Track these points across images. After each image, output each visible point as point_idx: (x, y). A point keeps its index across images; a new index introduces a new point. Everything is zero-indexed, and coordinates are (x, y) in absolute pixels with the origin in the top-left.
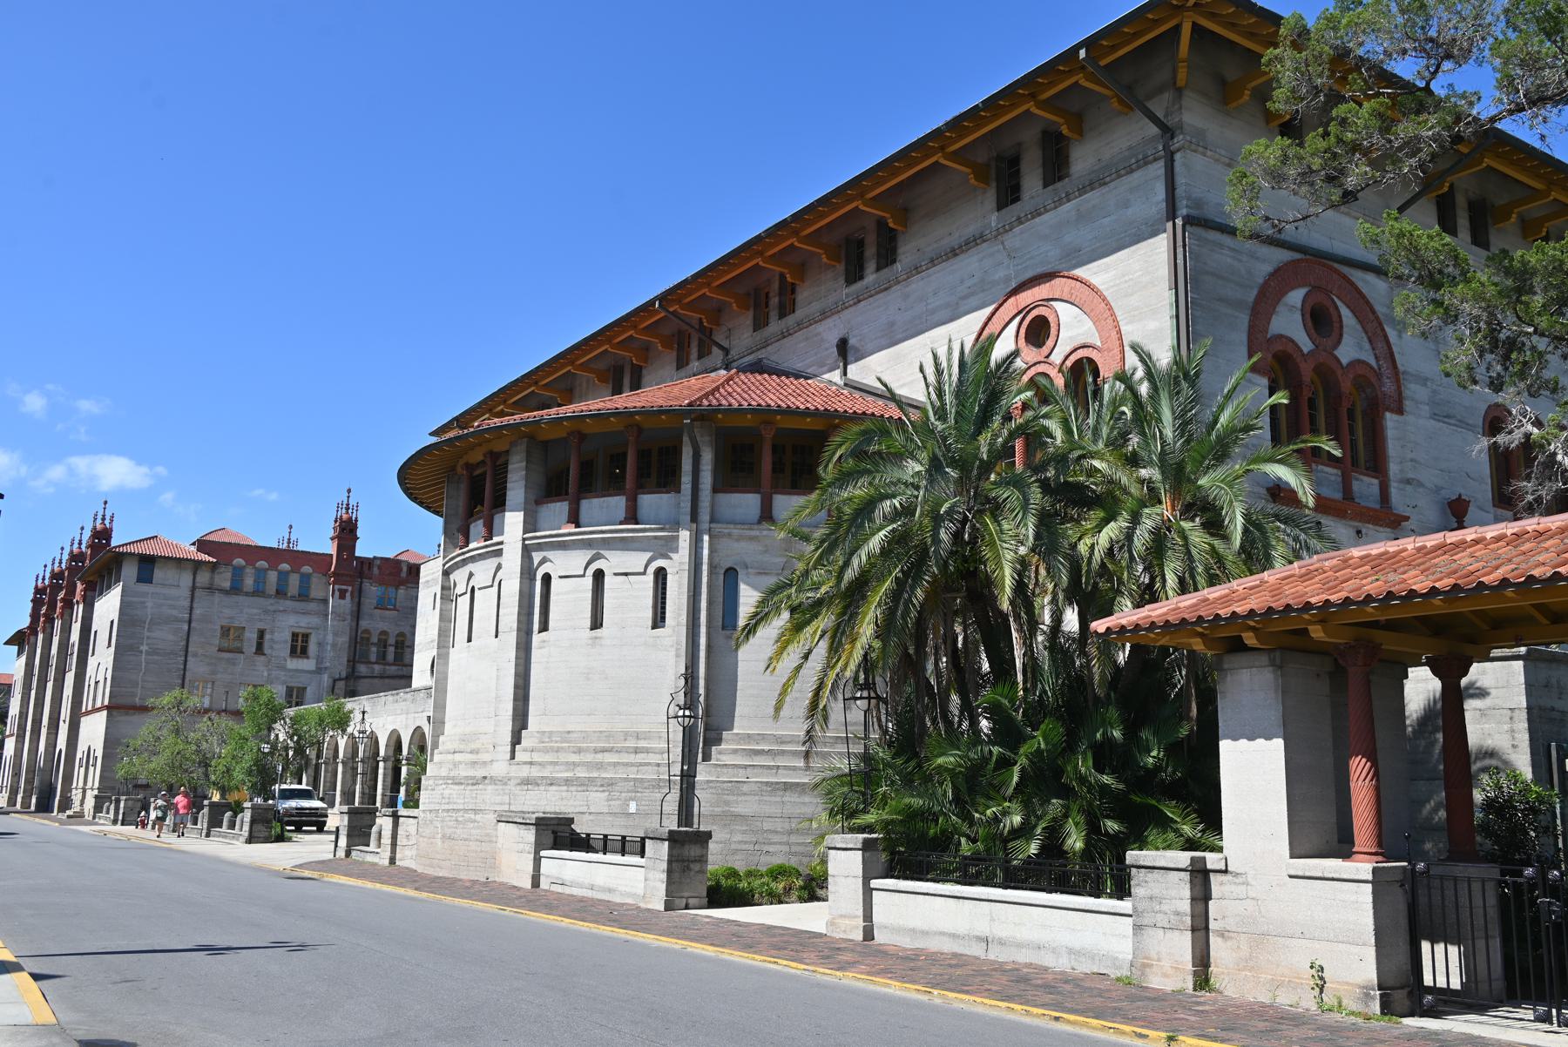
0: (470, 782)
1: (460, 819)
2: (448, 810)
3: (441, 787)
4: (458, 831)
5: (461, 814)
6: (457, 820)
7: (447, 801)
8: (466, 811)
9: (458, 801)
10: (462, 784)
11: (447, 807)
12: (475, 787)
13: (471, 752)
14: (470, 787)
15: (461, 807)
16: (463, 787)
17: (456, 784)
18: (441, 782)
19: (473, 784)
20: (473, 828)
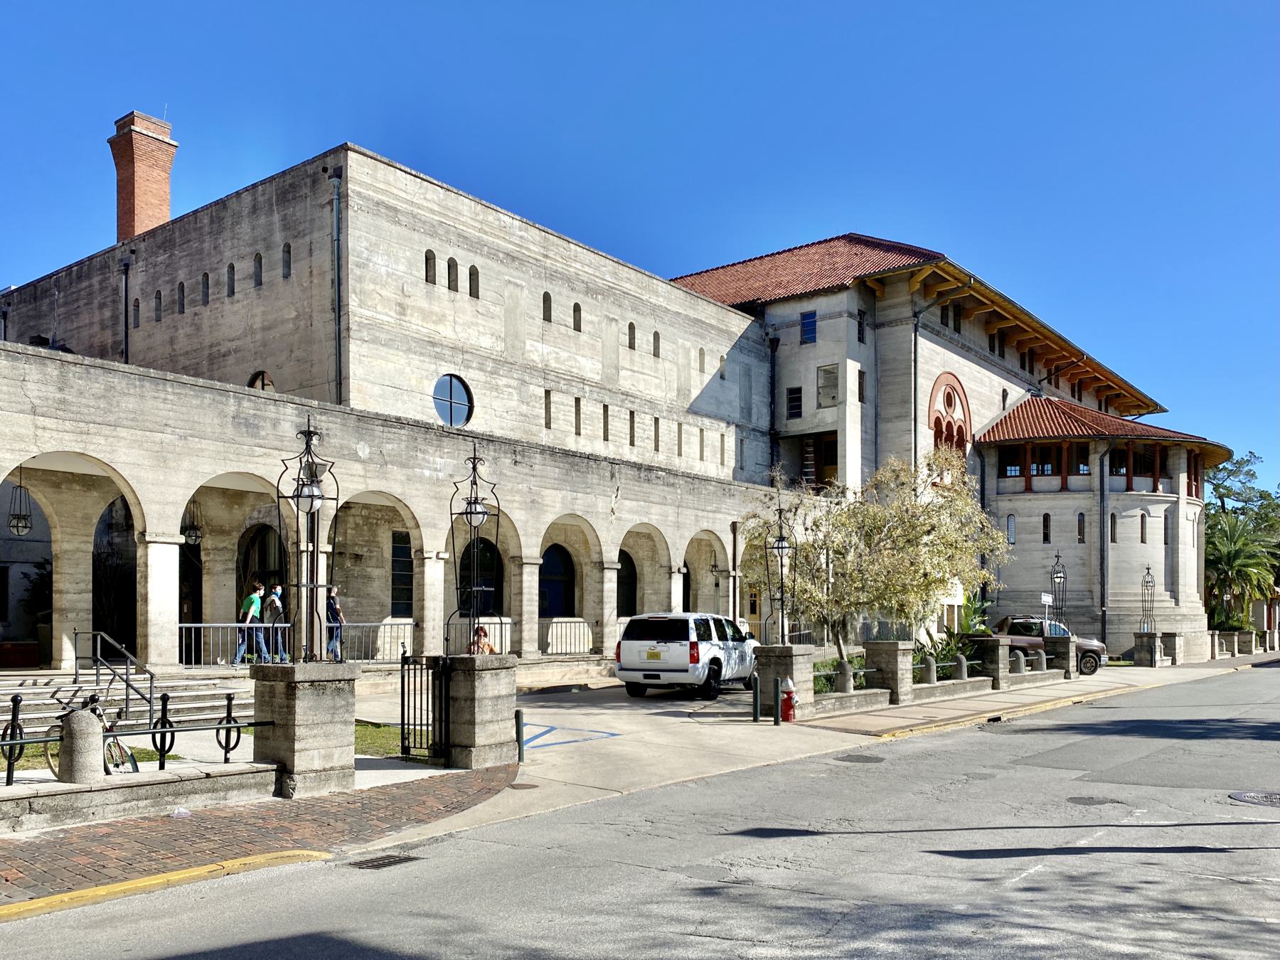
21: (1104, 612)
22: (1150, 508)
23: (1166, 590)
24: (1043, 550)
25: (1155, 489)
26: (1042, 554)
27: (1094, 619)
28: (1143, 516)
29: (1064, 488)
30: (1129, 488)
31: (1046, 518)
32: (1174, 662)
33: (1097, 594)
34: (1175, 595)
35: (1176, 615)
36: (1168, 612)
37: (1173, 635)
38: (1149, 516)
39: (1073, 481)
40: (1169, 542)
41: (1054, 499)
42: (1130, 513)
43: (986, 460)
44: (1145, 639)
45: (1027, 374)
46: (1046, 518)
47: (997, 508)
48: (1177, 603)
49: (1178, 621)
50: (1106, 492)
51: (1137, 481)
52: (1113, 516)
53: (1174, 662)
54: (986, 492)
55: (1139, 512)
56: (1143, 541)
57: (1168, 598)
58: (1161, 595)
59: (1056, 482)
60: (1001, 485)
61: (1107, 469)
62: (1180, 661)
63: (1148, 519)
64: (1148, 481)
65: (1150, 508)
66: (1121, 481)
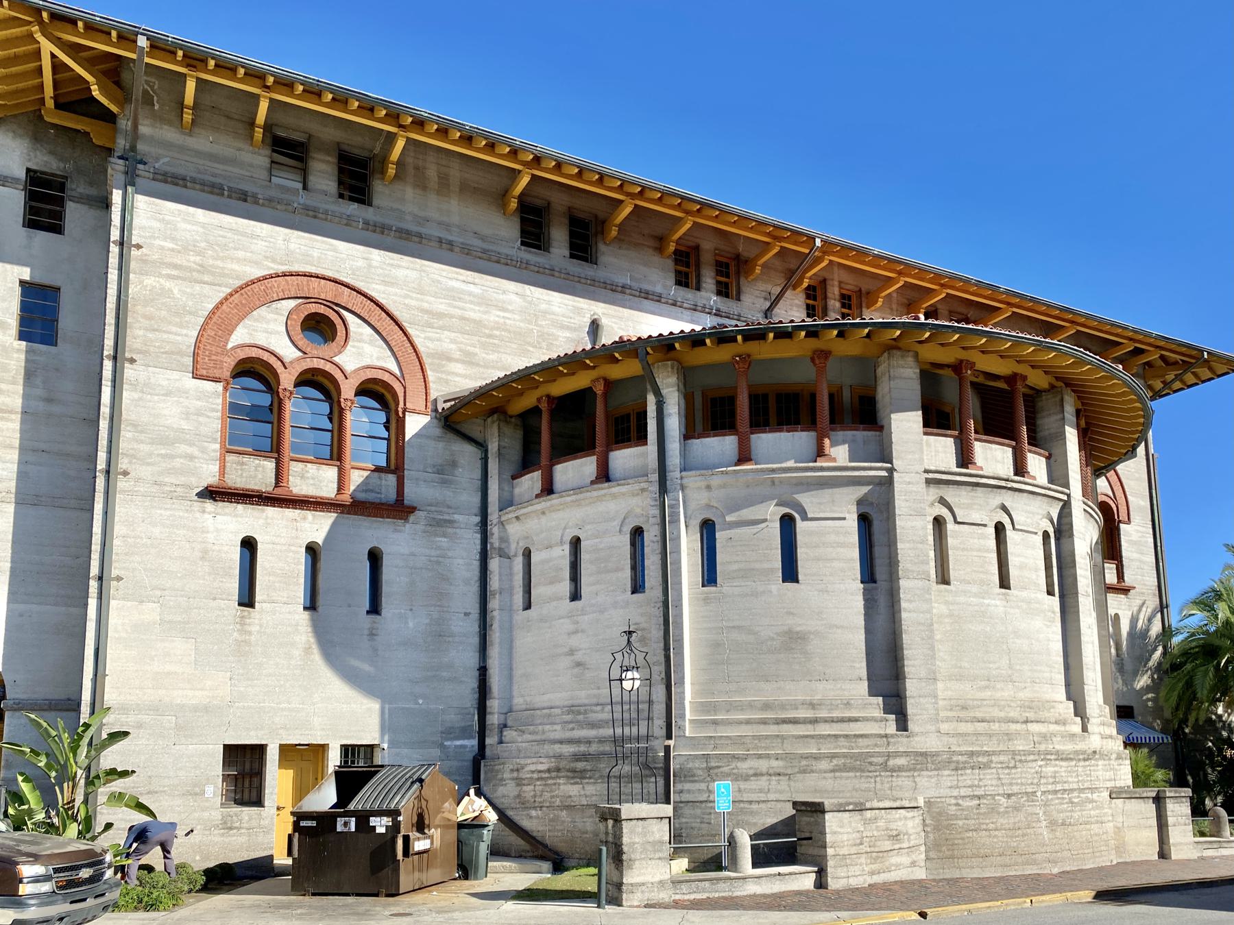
0: (1081, 757)
1: (1076, 800)
2: (1056, 792)
3: (1034, 764)
4: (1076, 815)
5: (1076, 794)
6: (1072, 803)
7: (1051, 780)
8: (1081, 790)
9: (1070, 779)
10: (1071, 759)
11: (1050, 787)
12: (1087, 763)
13: (1056, 723)
14: (1082, 763)
15: (1075, 786)
16: (1073, 763)
17: (1062, 759)
18: (1032, 757)
19: (1085, 760)
20: (1093, 809)
21: (667, 749)
22: (806, 499)
23: (873, 692)
24: (570, 616)
25: (820, 453)
26: (567, 625)
27: (647, 767)
28: (787, 523)
29: (604, 475)
30: (744, 457)
31: (576, 543)
32: (821, 884)
33: (660, 708)
34: (896, 704)
35: (889, 756)
36: (862, 746)
37: (817, 809)
38: (805, 518)
39: (622, 458)
40: (881, 572)
41: (577, 504)
42: (747, 514)
43: (490, 447)
44: (610, 822)
45: (714, 299)
46: (576, 543)
47: (504, 539)
48: (903, 724)
49: (900, 769)
50: (674, 474)
51: (764, 441)
52: (708, 529)
53: (821, 884)
54: (489, 511)
55: (773, 512)
56: (790, 573)
57: (878, 713)
58: (848, 704)
59: (586, 466)
60: (517, 491)
61: (674, 423)
62: (837, 879)
63: (801, 525)
64: (801, 439)
65: (806, 499)
66: (726, 444)
